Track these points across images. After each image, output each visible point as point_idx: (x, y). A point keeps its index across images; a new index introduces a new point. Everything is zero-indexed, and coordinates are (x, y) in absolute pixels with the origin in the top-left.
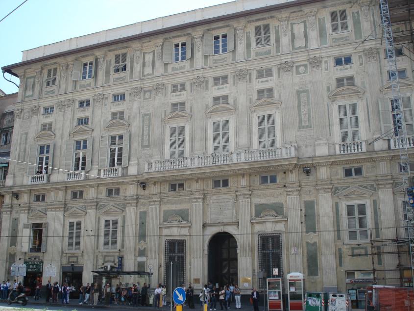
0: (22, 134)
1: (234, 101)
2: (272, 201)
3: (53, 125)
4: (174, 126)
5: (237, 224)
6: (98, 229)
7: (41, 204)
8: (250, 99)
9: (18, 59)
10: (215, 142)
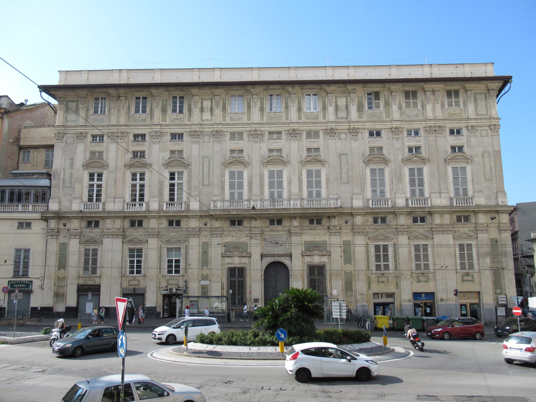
0: (65, 159)
1: (287, 155)
2: (318, 239)
3: (104, 154)
4: (233, 170)
5: (290, 256)
6: (161, 256)
7: (94, 230)
8: (301, 155)
9: (55, 81)
10: (270, 188)
